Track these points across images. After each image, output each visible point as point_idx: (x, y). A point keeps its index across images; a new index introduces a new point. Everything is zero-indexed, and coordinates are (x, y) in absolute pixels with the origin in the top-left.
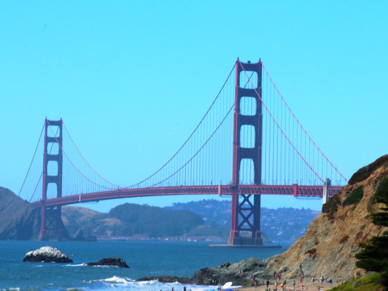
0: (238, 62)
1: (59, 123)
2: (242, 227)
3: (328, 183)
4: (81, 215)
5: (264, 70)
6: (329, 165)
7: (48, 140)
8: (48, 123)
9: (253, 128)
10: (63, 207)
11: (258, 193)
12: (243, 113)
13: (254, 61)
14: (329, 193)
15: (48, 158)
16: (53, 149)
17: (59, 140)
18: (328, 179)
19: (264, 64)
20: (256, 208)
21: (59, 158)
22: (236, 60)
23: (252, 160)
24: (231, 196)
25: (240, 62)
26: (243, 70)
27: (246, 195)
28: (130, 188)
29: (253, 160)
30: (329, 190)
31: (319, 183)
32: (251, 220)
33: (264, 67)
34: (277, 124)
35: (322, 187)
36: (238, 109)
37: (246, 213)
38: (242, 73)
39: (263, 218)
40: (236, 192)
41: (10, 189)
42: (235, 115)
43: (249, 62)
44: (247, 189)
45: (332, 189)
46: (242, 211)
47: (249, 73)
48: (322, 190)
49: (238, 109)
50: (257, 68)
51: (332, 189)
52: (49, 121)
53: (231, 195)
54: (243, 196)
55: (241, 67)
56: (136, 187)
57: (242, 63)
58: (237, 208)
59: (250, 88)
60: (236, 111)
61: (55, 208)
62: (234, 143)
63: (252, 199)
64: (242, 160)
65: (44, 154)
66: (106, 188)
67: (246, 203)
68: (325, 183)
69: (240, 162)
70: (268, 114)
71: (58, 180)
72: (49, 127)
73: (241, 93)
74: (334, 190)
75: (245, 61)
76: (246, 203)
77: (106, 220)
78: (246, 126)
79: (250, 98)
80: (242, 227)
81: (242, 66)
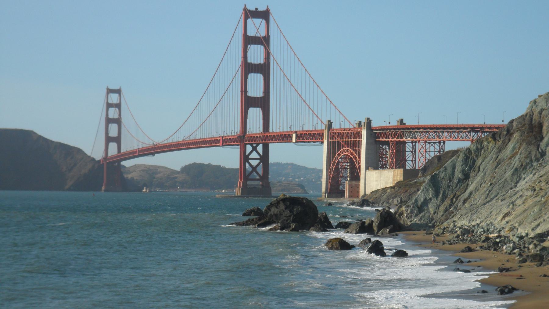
0: (245, 9)
1: (118, 91)
2: (250, 177)
3: (328, 125)
4: (160, 172)
5: (272, 17)
6: (338, 113)
7: (109, 106)
8: (110, 91)
9: (262, 76)
10: (123, 163)
11: (263, 141)
12: (249, 61)
13: (262, 8)
14: (330, 136)
15: (109, 121)
16: (113, 113)
17: (118, 106)
18: (329, 121)
19: (272, 11)
20: (264, 158)
21: (118, 121)
22: (243, 7)
23: (260, 109)
24: (239, 147)
25: (247, 10)
26: (249, 18)
27: (254, 145)
28: (162, 143)
29: (262, 110)
30: (331, 133)
31: (321, 127)
32: (260, 170)
33: (271, 13)
34: (276, 62)
35: (323, 130)
36: (245, 57)
37: (254, 163)
38: (249, 20)
39: (270, 169)
40: (244, 142)
41: (81, 148)
42: (242, 62)
43: (257, 9)
44: (254, 140)
45: (333, 132)
46: (250, 161)
47: (258, 21)
48: (323, 134)
49: (245, 57)
50: (265, 15)
51: (333, 132)
52: (110, 90)
53: (238, 145)
54: (251, 145)
55: (249, 14)
56: (166, 142)
57: (249, 11)
58: (245, 158)
59: (259, 36)
60: (243, 59)
61: (116, 164)
62: (242, 92)
63: (260, 148)
64: (250, 108)
65: (106, 118)
66: (146, 144)
67: (254, 152)
68: (326, 125)
69: (248, 111)
70: (275, 63)
71: (118, 140)
72: (109, 95)
73: (248, 41)
74: (335, 133)
75: (254, 9)
76: (254, 152)
77: (177, 175)
78: (252, 74)
79: (259, 46)
80: (250, 177)
81: (248, 13)
